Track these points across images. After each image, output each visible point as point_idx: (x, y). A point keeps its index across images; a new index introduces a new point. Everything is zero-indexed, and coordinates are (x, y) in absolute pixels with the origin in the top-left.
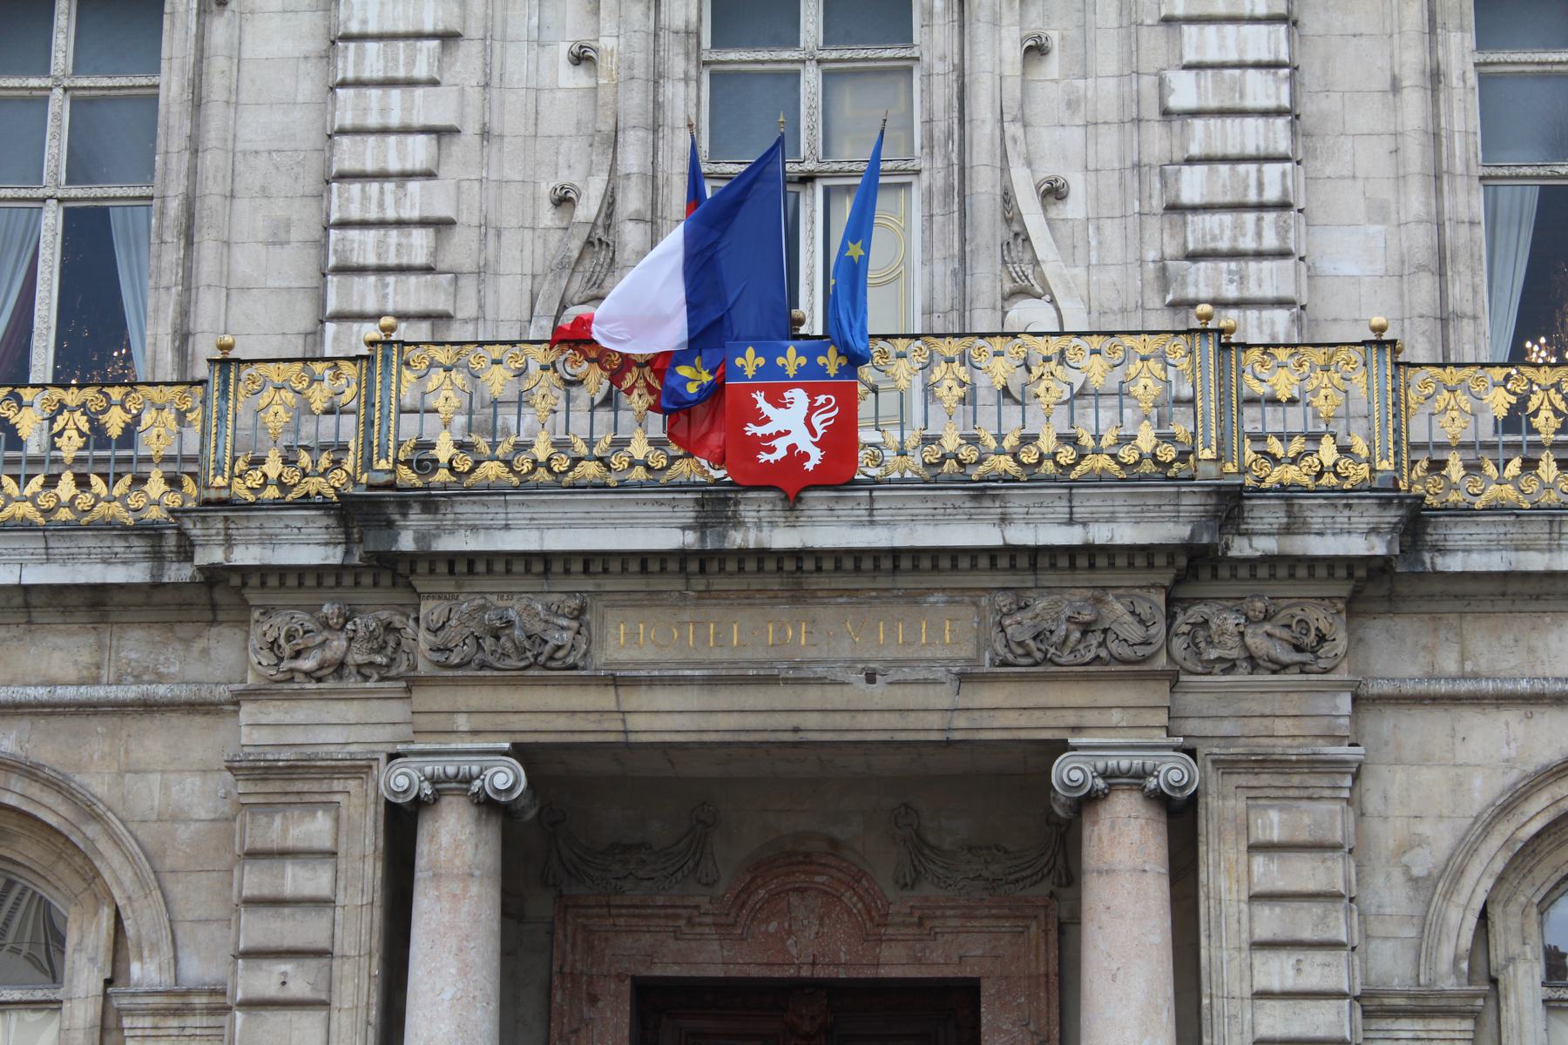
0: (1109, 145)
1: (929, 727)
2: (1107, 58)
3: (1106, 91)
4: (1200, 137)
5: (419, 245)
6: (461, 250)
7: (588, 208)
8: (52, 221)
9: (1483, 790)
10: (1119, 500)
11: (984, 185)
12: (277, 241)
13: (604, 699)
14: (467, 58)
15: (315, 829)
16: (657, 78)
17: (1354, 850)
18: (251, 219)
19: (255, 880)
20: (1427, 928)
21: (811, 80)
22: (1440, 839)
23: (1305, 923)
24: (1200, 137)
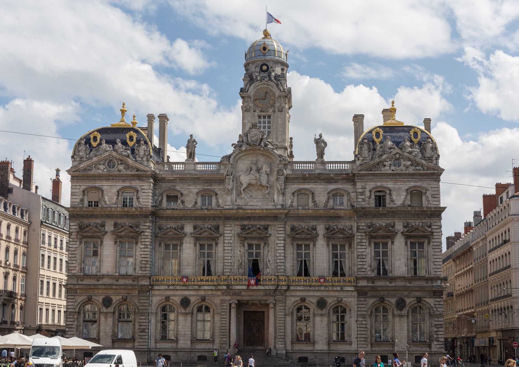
0: (273, 258)
2: (273, 252)
3: (273, 254)
4: (278, 258)
5: (230, 264)
6: (232, 264)
7: (240, 262)
9: (293, 302)
10: (271, 286)
11: (265, 261)
13: (241, 297)
14: (232, 252)
16: (245, 253)
17: (285, 306)
18: (219, 261)
19: (222, 308)
20: (289, 310)
22: (290, 305)
23: (282, 311)
24: (278, 258)
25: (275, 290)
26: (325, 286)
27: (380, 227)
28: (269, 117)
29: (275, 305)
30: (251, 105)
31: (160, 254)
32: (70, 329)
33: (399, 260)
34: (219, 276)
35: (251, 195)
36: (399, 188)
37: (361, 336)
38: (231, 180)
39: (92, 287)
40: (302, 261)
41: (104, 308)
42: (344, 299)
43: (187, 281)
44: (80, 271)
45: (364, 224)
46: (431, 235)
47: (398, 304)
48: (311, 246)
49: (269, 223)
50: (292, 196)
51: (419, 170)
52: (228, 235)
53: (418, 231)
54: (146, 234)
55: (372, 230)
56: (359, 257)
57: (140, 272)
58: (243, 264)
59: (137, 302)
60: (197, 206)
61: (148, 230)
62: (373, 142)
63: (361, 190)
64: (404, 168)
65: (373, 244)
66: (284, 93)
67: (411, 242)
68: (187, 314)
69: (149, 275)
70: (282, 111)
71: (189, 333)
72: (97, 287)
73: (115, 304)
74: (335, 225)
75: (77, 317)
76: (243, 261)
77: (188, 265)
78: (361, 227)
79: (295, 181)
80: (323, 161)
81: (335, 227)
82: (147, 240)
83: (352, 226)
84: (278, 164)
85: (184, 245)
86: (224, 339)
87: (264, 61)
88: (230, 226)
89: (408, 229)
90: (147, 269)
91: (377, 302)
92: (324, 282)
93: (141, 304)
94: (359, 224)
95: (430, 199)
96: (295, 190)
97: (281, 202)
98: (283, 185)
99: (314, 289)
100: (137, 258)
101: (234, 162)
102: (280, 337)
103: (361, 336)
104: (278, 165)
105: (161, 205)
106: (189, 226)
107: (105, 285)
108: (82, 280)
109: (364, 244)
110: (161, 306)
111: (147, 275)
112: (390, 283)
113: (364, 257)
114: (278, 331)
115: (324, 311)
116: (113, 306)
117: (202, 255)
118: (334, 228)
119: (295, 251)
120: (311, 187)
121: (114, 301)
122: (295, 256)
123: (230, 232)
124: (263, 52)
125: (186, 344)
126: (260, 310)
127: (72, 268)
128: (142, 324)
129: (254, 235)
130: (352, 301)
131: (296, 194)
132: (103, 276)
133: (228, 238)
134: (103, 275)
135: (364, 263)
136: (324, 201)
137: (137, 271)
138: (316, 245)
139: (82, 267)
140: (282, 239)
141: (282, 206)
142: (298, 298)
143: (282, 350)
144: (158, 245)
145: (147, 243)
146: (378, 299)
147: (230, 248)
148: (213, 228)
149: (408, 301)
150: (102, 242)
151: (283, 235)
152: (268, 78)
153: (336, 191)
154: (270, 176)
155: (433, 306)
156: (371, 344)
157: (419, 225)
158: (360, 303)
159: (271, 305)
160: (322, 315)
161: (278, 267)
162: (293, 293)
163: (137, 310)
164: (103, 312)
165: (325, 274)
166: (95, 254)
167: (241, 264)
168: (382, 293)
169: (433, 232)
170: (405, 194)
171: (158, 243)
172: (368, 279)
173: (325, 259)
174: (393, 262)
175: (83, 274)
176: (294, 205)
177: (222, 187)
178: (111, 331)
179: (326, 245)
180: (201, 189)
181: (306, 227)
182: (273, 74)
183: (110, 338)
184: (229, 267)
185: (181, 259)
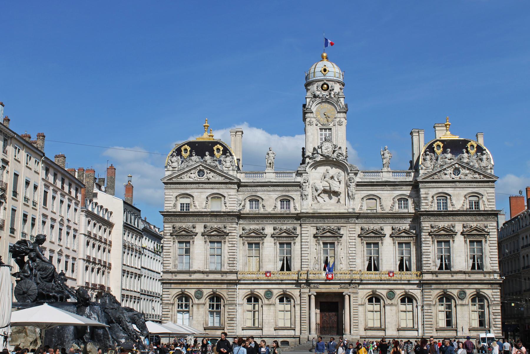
0: (346, 255)
1: (337, 291)
2: (346, 250)
3: (346, 251)
4: (351, 255)
5: (307, 260)
6: (309, 260)
7: (317, 258)
8: (285, 257)
9: (365, 294)
11: (339, 258)
12: (299, 259)
14: (309, 249)
15: (305, 296)
21: (329, 250)
22: (363, 296)
24: (351, 255)
25: (350, 284)
26: (395, 280)
27: (443, 227)
28: (330, 129)
29: (349, 296)
30: (313, 119)
31: (244, 252)
32: (166, 319)
33: (460, 256)
34: (299, 271)
36: (459, 193)
37: (427, 323)
39: (186, 281)
40: (371, 257)
41: (196, 299)
42: (410, 291)
43: (270, 276)
44: (174, 267)
45: (427, 225)
46: (488, 235)
47: (460, 295)
48: (380, 244)
49: (342, 225)
51: (476, 178)
52: (305, 235)
53: (475, 231)
54: (233, 234)
55: (435, 231)
56: (424, 254)
57: (229, 268)
58: (319, 260)
59: (225, 295)
60: (276, 209)
61: (235, 231)
62: (434, 152)
63: (425, 196)
64: (463, 177)
65: (436, 242)
66: (344, 109)
67: (470, 241)
68: (270, 305)
69: (236, 270)
70: (342, 125)
71: (272, 321)
72: (190, 281)
73: (207, 296)
74: (401, 226)
75: (172, 308)
76: (319, 258)
77: (270, 261)
78: (425, 228)
81: (401, 228)
82: (234, 240)
83: (415, 226)
85: (265, 244)
86: (304, 327)
87: (325, 81)
88: (307, 227)
89: (467, 229)
90: (235, 265)
91: (441, 293)
92: (393, 276)
93: (230, 296)
94: (423, 225)
95: (486, 203)
97: (352, 206)
98: (354, 191)
99: (384, 282)
100: (225, 256)
102: (354, 324)
103: (427, 323)
105: (244, 209)
106: (269, 227)
107: (197, 280)
108: (176, 276)
109: (428, 242)
110: (247, 297)
111: (234, 270)
112: (452, 276)
113: (428, 254)
114: (352, 319)
115: (393, 301)
116: (204, 298)
117: (282, 252)
118: (400, 229)
119: (365, 249)
121: (205, 294)
122: (365, 253)
123: (306, 232)
125: (270, 331)
126: (334, 301)
127: (167, 265)
128: (230, 313)
129: (328, 234)
130: (418, 292)
131: (365, 199)
132: (195, 272)
133: (305, 238)
134: (195, 271)
135: (428, 259)
136: (391, 205)
137: (225, 267)
138: (384, 244)
139: (176, 263)
140: (354, 238)
141: (354, 209)
142: (370, 290)
143: (357, 335)
144: (242, 245)
145: (234, 242)
146: (442, 290)
147: (307, 246)
148: (291, 229)
149: (468, 292)
150: (193, 241)
151: (354, 235)
152: (329, 96)
153: (401, 196)
155: (491, 296)
156: (436, 330)
157: (477, 225)
158: (425, 294)
159: (347, 297)
160: (392, 305)
161: (351, 263)
162: (366, 286)
163: (225, 301)
164: (195, 304)
165: (392, 269)
166: (188, 251)
167: (317, 261)
168: (445, 286)
169: (489, 232)
170: (464, 198)
171: (242, 242)
172: (432, 273)
173: (392, 255)
174: (454, 258)
175: (176, 270)
176: (363, 209)
178: (203, 319)
179: (393, 244)
180: (280, 195)
181: (375, 228)
182: (332, 93)
183: (202, 326)
184: (306, 263)
185: (264, 256)
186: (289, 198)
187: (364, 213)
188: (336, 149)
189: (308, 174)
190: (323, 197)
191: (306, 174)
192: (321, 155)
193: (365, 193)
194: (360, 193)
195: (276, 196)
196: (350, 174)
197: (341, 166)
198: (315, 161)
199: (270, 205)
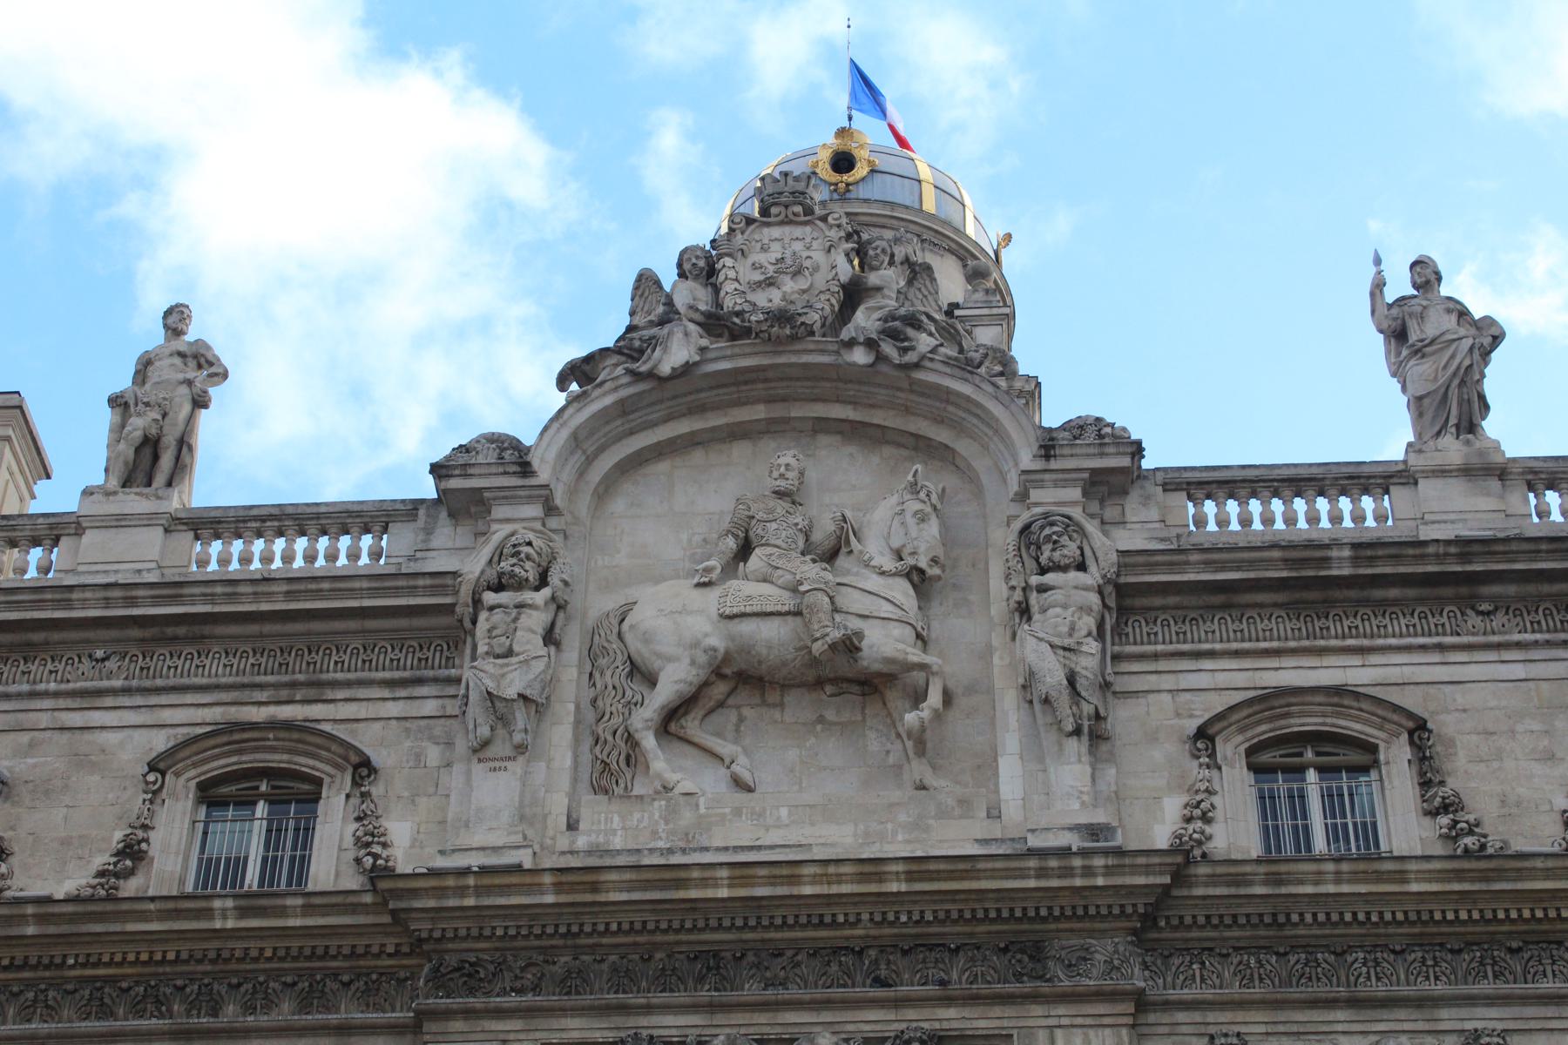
35: (741, 769)
38: (536, 621)
50: (1194, 770)
79: (1215, 632)
80: (1481, 453)
84: (1030, 480)
96: (1219, 703)
101: (573, 492)
104: (1022, 497)
120: (1394, 674)
124: (835, 177)
131: (1231, 748)
141: (1093, 831)
154: (936, 609)
177: (430, 707)
186: (304, 764)
187: (1233, 872)
188: (873, 279)
189: (551, 509)
190: (725, 748)
191: (534, 510)
192: (716, 323)
193: (1222, 679)
194: (1167, 682)
195: (160, 742)
196: (1035, 495)
197: (942, 435)
198: (637, 376)
199: (66, 842)
